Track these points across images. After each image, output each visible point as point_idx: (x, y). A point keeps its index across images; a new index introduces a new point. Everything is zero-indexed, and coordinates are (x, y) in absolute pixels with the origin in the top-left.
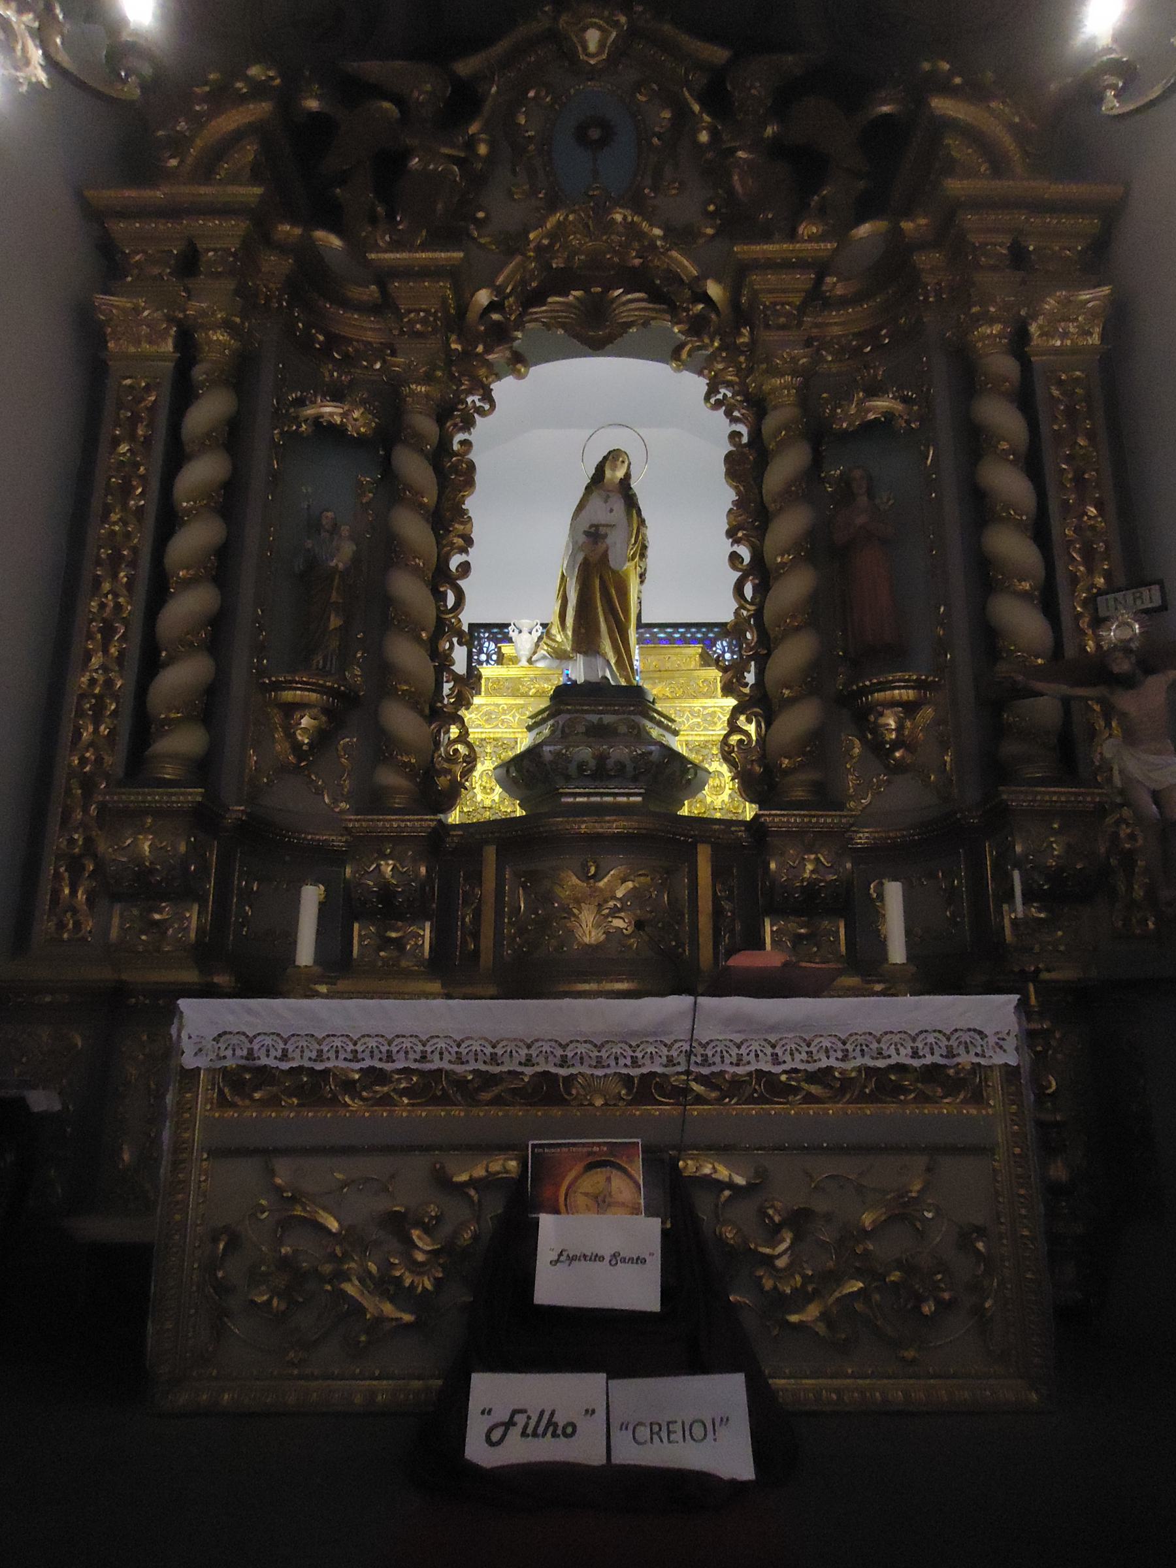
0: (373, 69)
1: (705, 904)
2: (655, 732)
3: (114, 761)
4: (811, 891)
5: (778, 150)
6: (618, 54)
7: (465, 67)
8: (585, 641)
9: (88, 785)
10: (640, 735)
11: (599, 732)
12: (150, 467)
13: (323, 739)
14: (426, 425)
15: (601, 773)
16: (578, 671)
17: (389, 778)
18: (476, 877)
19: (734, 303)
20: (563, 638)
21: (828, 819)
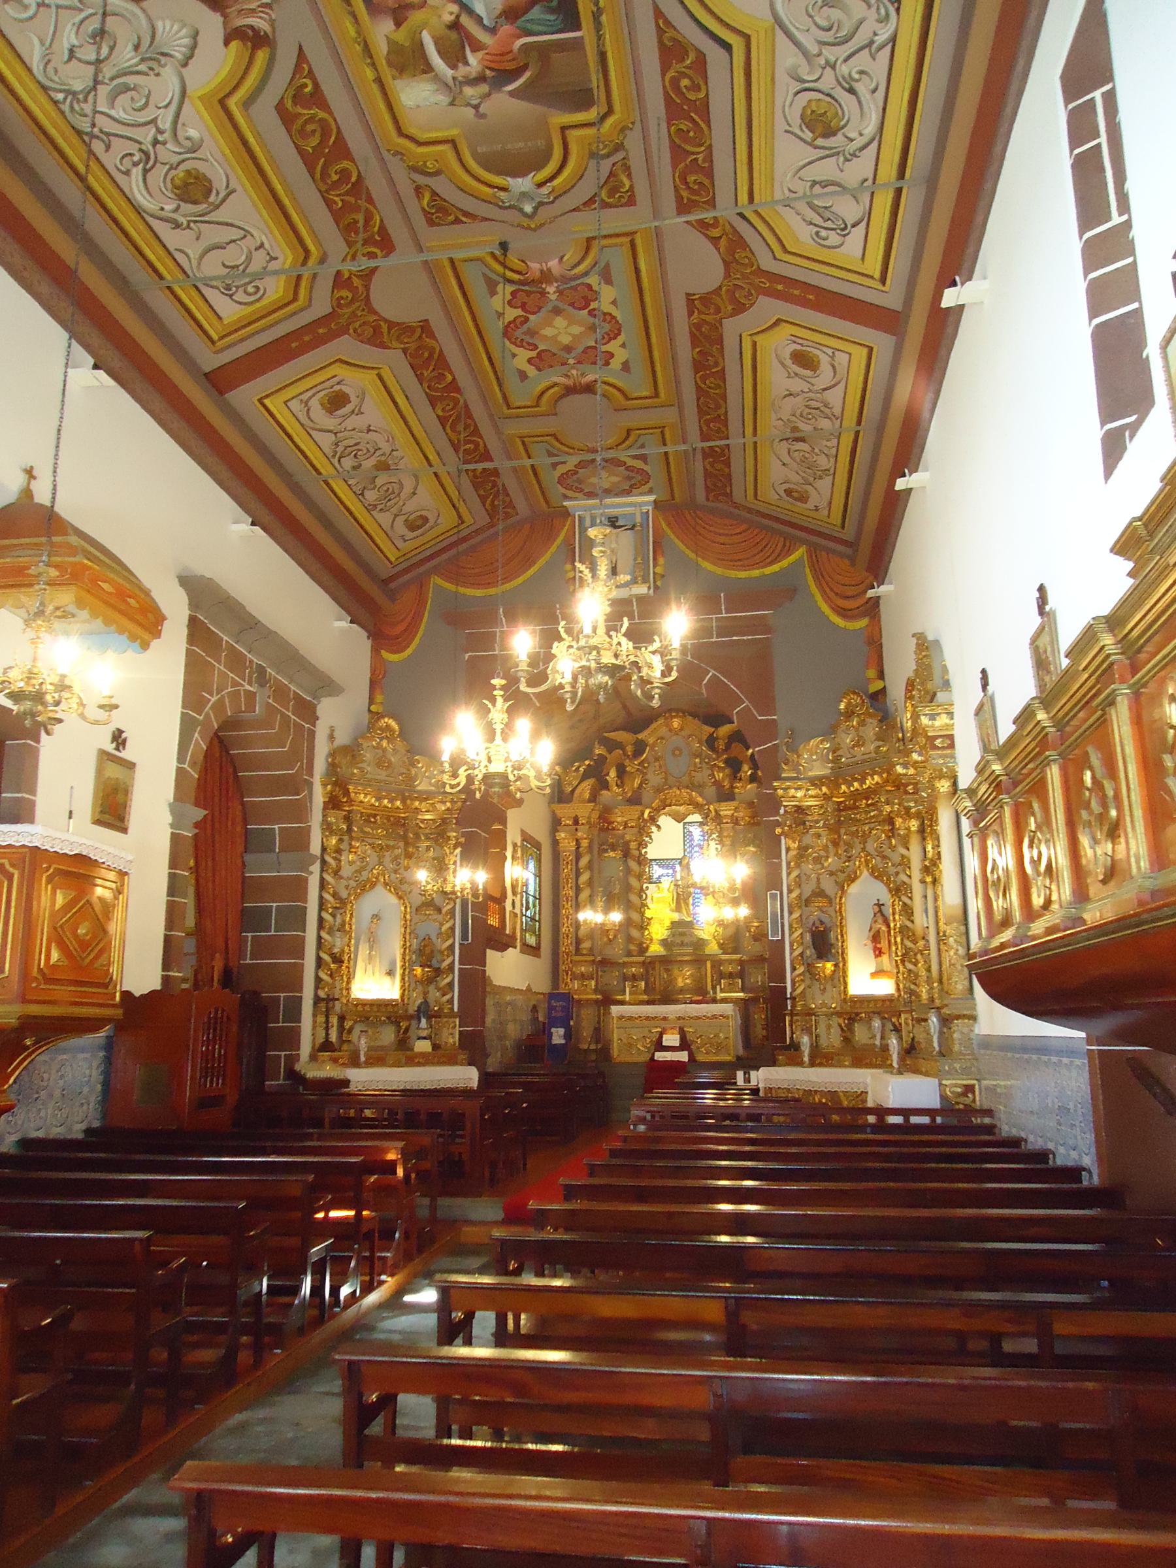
0: (612, 735)
1: (709, 975)
2: (696, 932)
3: (572, 949)
4: (731, 973)
5: (726, 762)
6: (682, 729)
7: (640, 736)
8: (678, 909)
9: (567, 954)
10: (692, 935)
11: (682, 934)
12: (573, 876)
13: (615, 937)
14: (636, 853)
15: (682, 944)
16: (676, 917)
17: (632, 947)
18: (654, 969)
19: (716, 811)
20: (673, 906)
21: (735, 957)
